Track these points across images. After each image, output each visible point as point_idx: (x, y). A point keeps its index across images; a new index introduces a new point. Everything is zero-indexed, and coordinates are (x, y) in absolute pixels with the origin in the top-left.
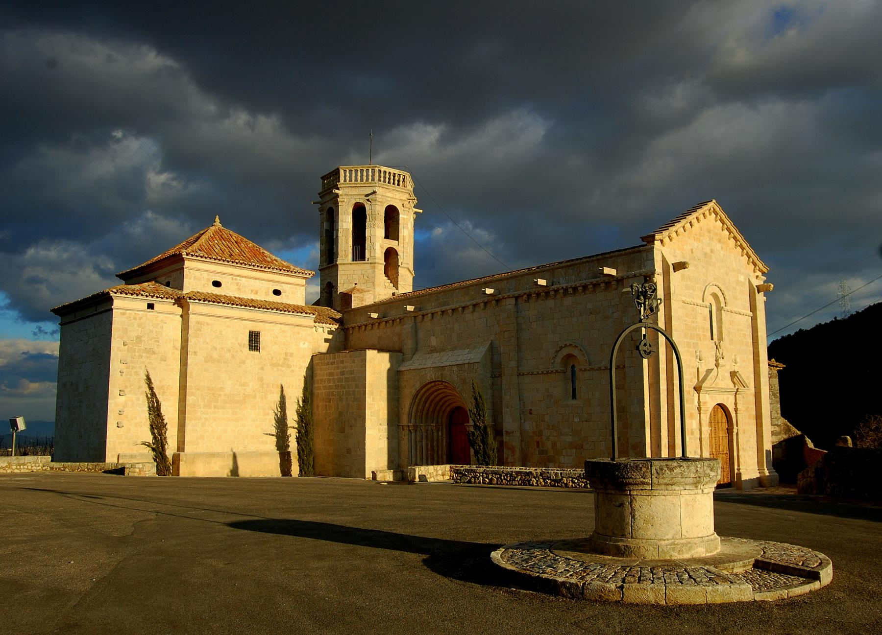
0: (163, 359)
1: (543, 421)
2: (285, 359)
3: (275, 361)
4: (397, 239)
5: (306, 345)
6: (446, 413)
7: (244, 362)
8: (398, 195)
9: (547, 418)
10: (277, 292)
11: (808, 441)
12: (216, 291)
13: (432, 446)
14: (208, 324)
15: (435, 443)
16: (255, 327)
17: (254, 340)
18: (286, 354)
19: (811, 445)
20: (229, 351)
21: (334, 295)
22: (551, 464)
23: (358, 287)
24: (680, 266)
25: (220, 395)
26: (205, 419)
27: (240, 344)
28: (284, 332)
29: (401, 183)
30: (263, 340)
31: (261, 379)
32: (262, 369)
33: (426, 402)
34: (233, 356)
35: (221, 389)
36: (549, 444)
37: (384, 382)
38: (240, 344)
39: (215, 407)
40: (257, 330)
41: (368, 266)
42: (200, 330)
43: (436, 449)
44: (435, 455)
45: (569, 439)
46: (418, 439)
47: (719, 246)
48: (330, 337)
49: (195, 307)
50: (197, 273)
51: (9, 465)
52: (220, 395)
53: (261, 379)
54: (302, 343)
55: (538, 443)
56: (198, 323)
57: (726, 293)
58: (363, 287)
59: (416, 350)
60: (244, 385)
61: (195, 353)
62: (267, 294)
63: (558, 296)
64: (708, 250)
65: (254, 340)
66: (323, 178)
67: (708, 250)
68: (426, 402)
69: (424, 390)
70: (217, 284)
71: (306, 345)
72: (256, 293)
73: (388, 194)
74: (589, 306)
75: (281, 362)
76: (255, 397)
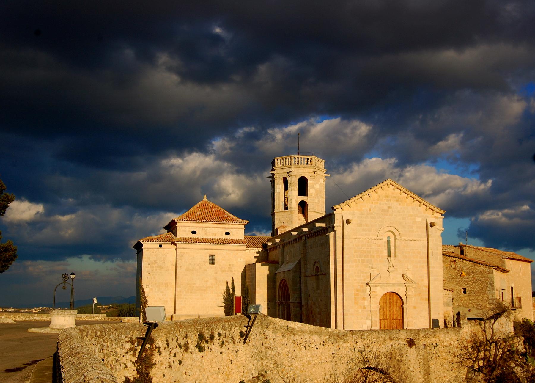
0: (167, 270)
5: (242, 260)
7: (206, 271)
8: (306, 170)
10: (227, 234)
12: (194, 236)
16: (212, 252)
17: (212, 259)
20: (198, 265)
24: (348, 222)
27: (204, 262)
29: (309, 163)
30: (217, 258)
31: (216, 279)
32: (216, 273)
33: (285, 290)
34: (200, 268)
35: (194, 284)
37: (266, 279)
38: (204, 262)
39: (191, 293)
40: (213, 254)
41: (289, 213)
47: (396, 204)
48: (258, 255)
49: (179, 245)
50: (184, 228)
51: (87, 317)
53: (216, 279)
54: (239, 259)
56: (182, 252)
57: (400, 230)
59: (283, 262)
60: (207, 281)
61: (180, 267)
62: (221, 235)
64: (385, 207)
65: (212, 259)
67: (385, 207)
70: (194, 232)
71: (242, 260)
72: (216, 235)
73: (300, 171)
75: (227, 269)
76: (213, 287)
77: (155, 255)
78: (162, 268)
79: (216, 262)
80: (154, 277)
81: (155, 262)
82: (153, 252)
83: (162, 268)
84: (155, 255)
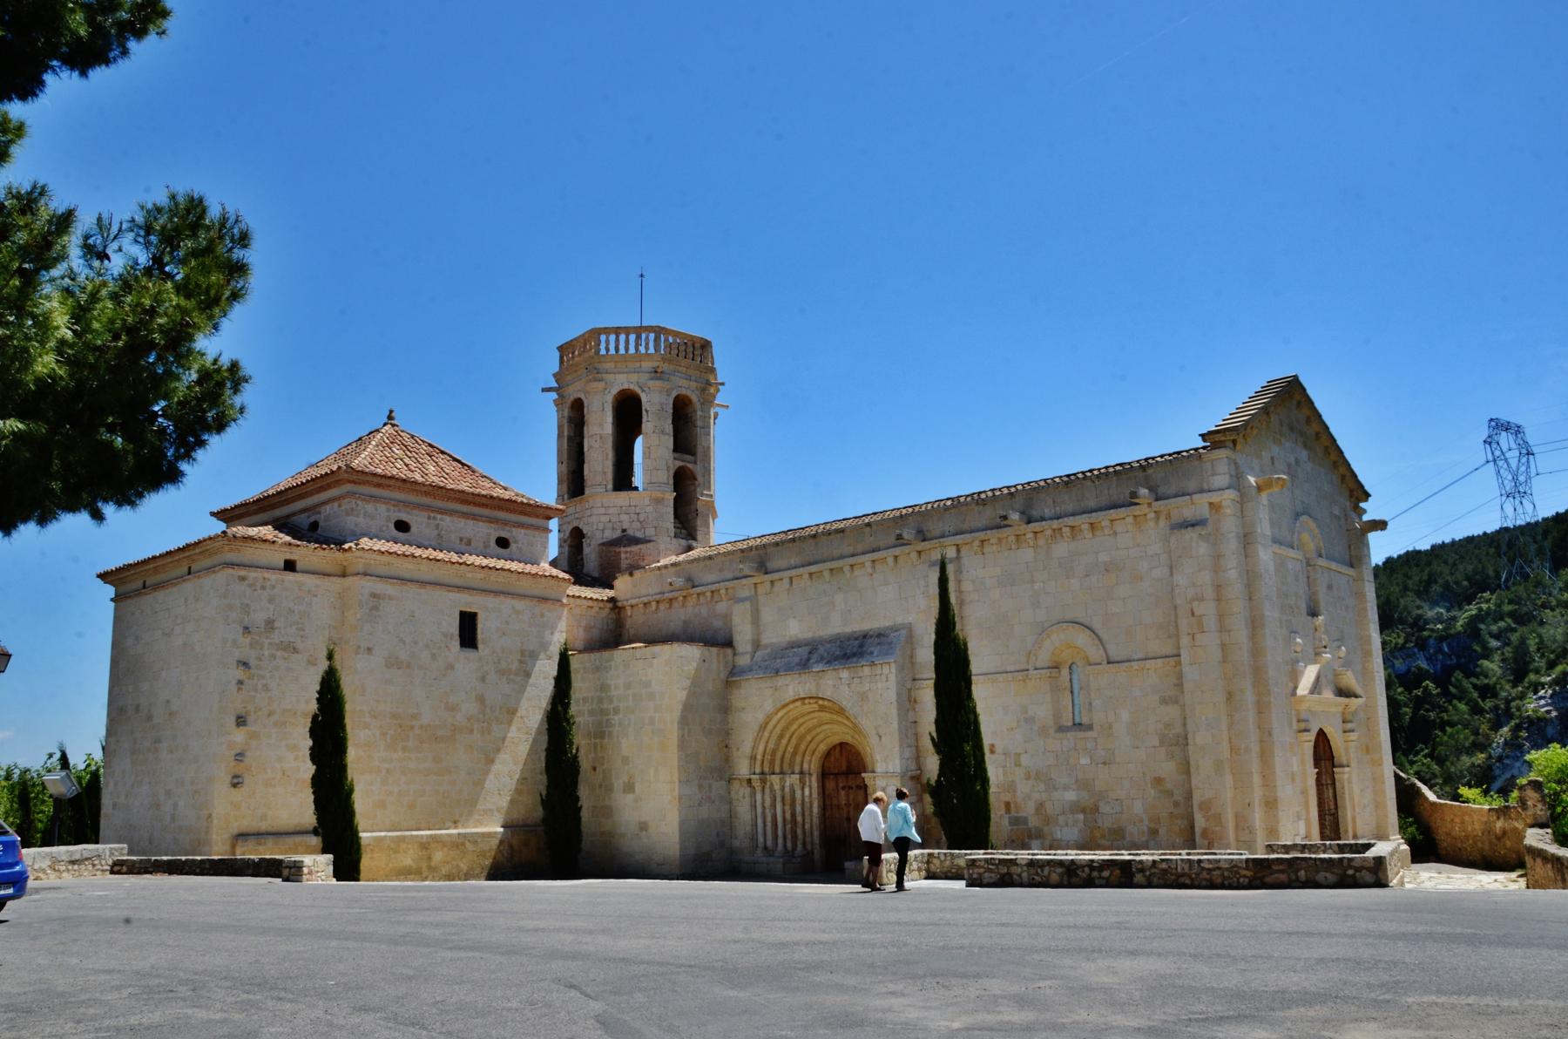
1: (1018, 764)
2: (521, 662)
3: (504, 665)
4: (693, 453)
6: (818, 755)
7: (450, 667)
9: (1025, 760)
11: (1425, 789)
13: (793, 815)
14: (391, 598)
15: (798, 809)
18: (523, 652)
19: (1432, 797)
20: (427, 646)
21: (586, 550)
22: (1035, 843)
23: (630, 532)
25: (412, 728)
26: (388, 771)
28: (518, 613)
30: (483, 628)
32: (483, 679)
34: (433, 656)
35: (414, 717)
36: (1028, 810)
42: (375, 608)
43: (799, 819)
44: (799, 831)
45: (1071, 796)
46: (768, 802)
50: (369, 507)
52: (412, 728)
53: (481, 699)
55: (1008, 805)
56: (374, 595)
58: (639, 535)
60: (452, 708)
63: (1041, 542)
66: (560, 348)
68: (781, 736)
69: (780, 714)
74: (1104, 557)
76: (472, 731)
77: (271, 601)
78: (295, 651)
79: (480, 636)
80: (266, 688)
81: (270, 625)
82: (263, 588)
83: (295, 651)
84: (271, 601)
